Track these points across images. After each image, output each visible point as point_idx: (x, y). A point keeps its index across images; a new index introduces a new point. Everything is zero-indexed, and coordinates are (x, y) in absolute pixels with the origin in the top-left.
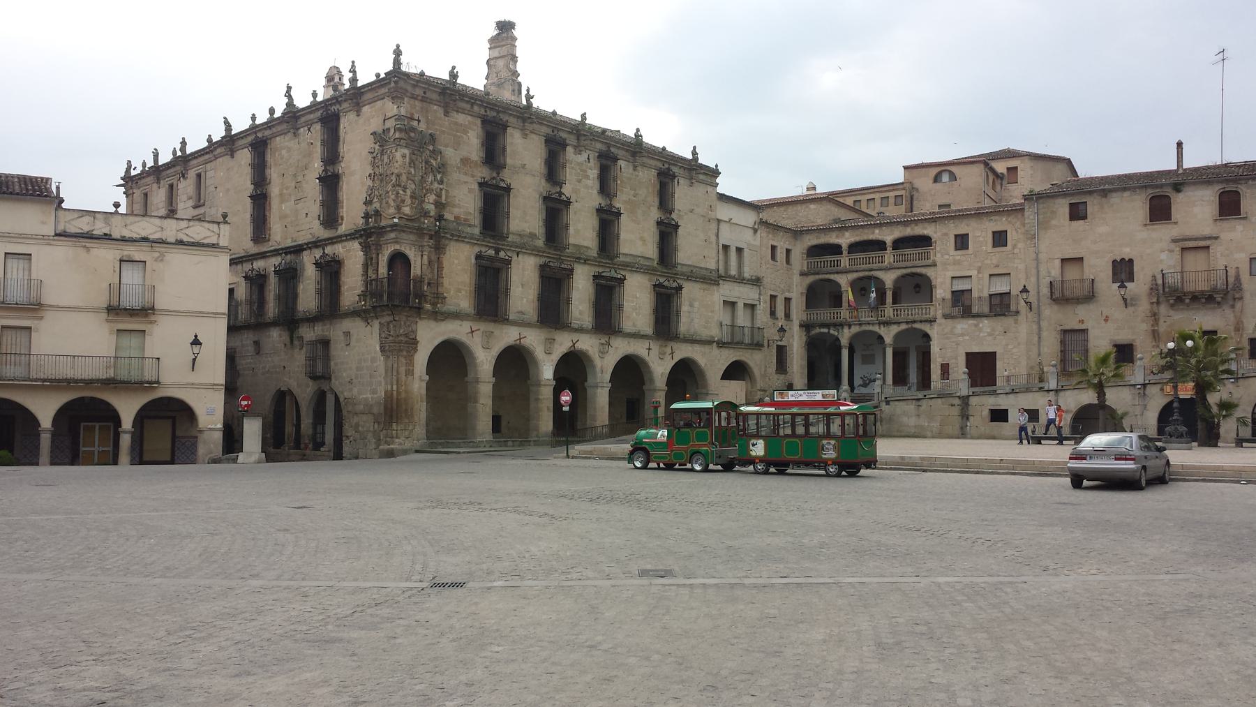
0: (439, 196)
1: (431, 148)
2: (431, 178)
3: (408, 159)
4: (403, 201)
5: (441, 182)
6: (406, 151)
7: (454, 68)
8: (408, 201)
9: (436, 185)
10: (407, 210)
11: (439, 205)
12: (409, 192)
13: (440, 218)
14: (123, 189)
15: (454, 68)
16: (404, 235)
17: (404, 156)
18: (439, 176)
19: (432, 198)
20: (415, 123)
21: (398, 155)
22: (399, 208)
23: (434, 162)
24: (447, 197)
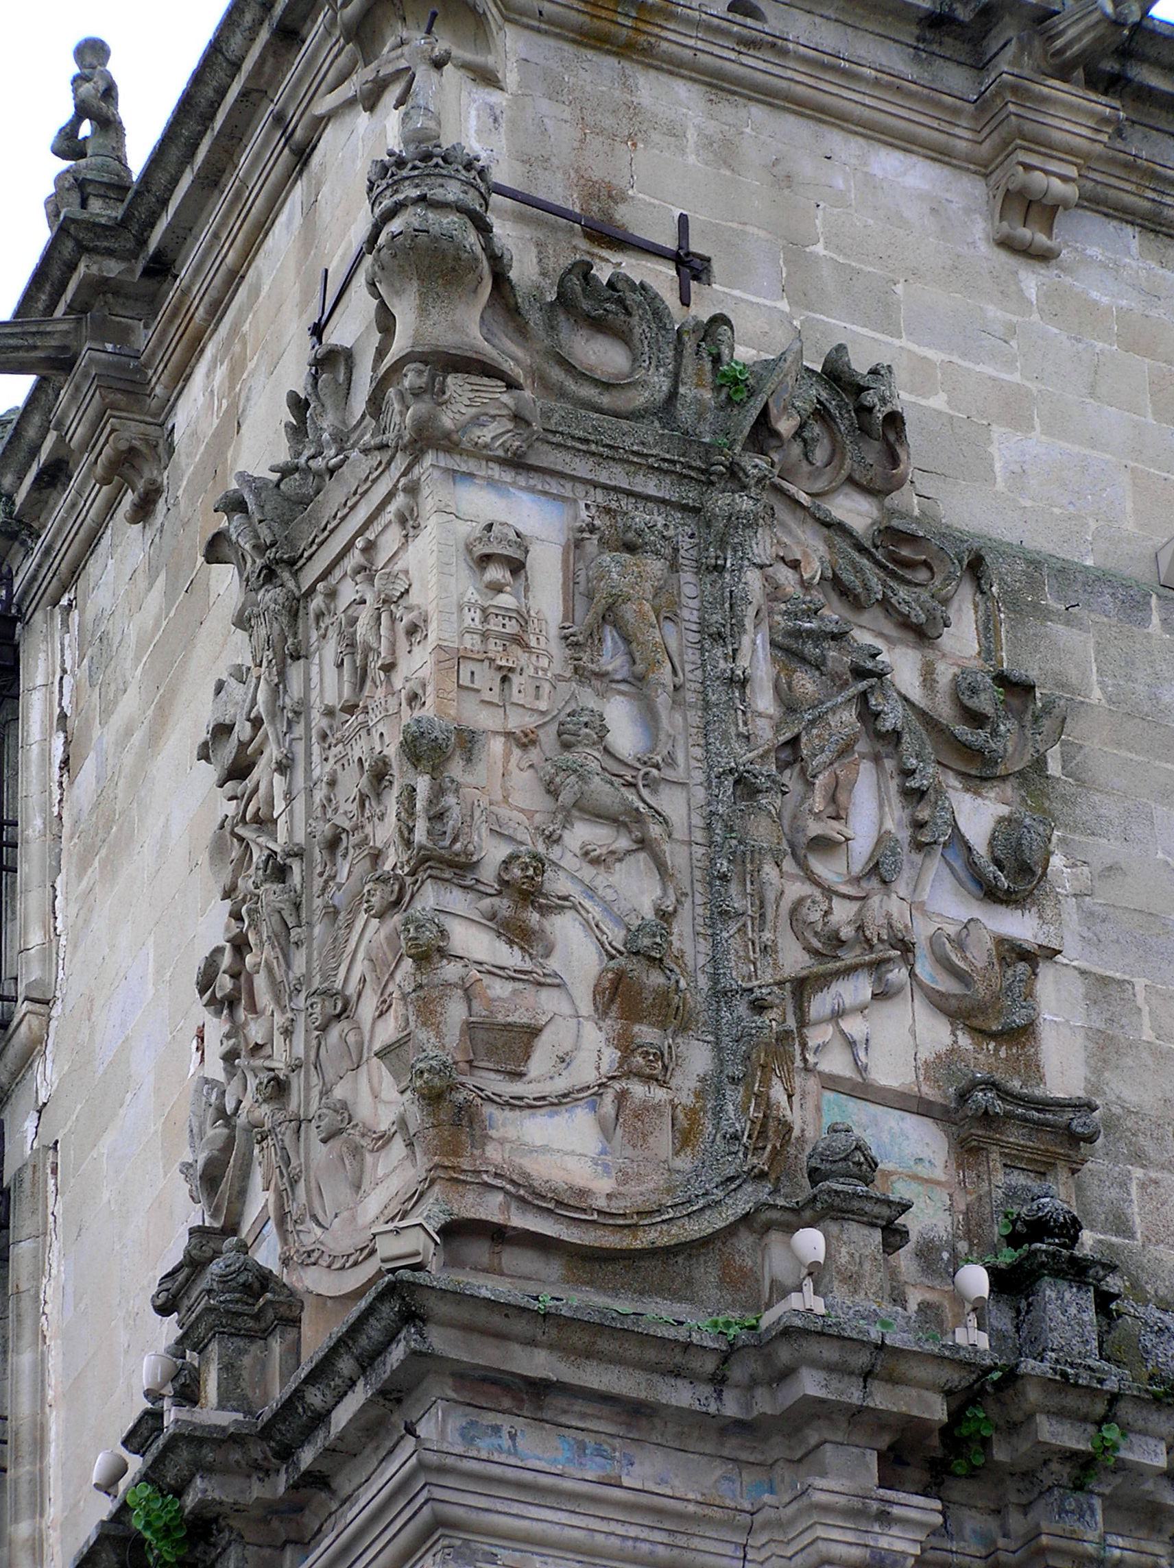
0: (994, 1009)
1: (855, 511)
2: (870, 813)
3: (546, 596)
4: (511, 1043)
5: (1011, 875)
6: (535, 519)
8: (578, 1043)
9: (939, 904)
10: (561, 1148)
11: (995, 1117)
12: (577, 951)
13: (1036, 1256)
16: (538, 1450)
17: (501, 559)
18: (977, 816)
19: (902, 1039)
21: (429, 565)
22: (449, 1114)
23: (904, 667)
24: (1104, 1048)
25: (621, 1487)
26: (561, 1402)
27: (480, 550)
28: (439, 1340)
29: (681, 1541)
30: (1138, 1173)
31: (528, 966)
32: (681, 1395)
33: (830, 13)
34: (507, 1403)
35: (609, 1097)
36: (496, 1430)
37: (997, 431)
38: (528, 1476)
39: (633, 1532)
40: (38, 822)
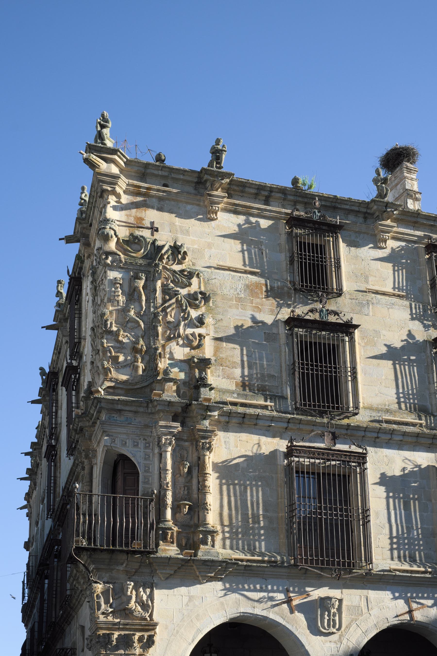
7: (218, 142)
14: (26, 511)
15: (218, 142)
20: (146, 234)
25: (131, 424)
26: (124, 412)
27: (114, 282)
28: (103, 405)
29: (142, 431)
30: (221, 368)
31: (120, 346)
32: (141, 410)
33: (180, 183)
34: (115, 413)
35: (132, 366)
36: (114, 417)
37: (206, 250)
38: (117, 424)
39: (134, 430)
40: (84, 310)
